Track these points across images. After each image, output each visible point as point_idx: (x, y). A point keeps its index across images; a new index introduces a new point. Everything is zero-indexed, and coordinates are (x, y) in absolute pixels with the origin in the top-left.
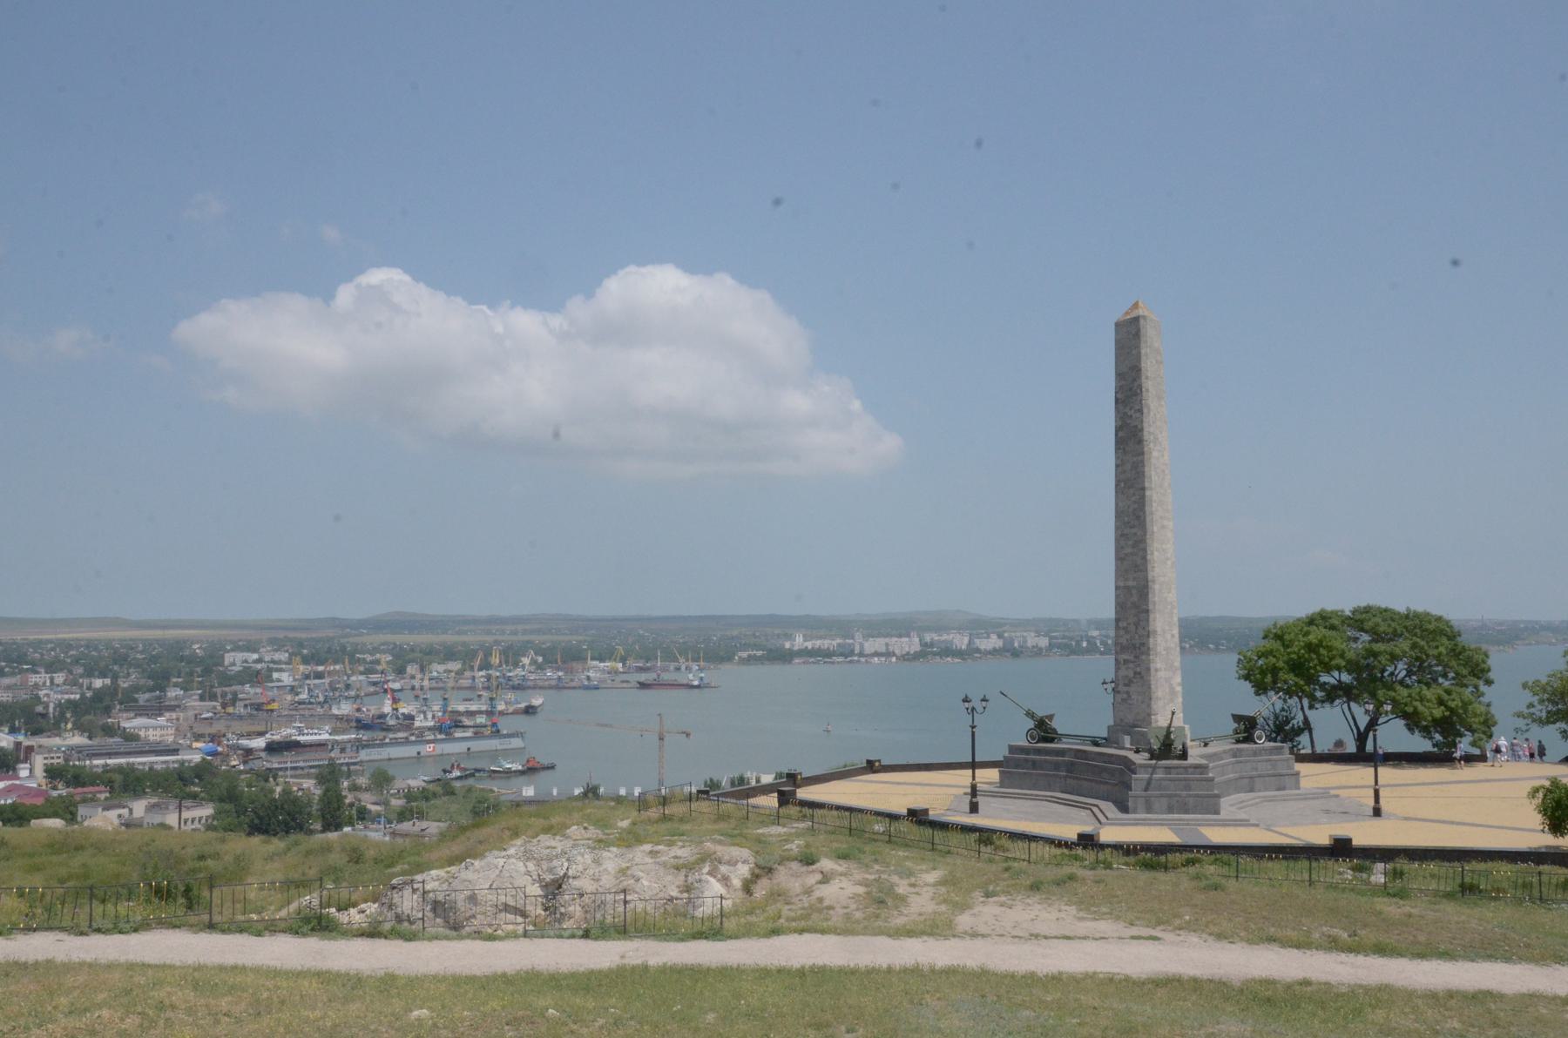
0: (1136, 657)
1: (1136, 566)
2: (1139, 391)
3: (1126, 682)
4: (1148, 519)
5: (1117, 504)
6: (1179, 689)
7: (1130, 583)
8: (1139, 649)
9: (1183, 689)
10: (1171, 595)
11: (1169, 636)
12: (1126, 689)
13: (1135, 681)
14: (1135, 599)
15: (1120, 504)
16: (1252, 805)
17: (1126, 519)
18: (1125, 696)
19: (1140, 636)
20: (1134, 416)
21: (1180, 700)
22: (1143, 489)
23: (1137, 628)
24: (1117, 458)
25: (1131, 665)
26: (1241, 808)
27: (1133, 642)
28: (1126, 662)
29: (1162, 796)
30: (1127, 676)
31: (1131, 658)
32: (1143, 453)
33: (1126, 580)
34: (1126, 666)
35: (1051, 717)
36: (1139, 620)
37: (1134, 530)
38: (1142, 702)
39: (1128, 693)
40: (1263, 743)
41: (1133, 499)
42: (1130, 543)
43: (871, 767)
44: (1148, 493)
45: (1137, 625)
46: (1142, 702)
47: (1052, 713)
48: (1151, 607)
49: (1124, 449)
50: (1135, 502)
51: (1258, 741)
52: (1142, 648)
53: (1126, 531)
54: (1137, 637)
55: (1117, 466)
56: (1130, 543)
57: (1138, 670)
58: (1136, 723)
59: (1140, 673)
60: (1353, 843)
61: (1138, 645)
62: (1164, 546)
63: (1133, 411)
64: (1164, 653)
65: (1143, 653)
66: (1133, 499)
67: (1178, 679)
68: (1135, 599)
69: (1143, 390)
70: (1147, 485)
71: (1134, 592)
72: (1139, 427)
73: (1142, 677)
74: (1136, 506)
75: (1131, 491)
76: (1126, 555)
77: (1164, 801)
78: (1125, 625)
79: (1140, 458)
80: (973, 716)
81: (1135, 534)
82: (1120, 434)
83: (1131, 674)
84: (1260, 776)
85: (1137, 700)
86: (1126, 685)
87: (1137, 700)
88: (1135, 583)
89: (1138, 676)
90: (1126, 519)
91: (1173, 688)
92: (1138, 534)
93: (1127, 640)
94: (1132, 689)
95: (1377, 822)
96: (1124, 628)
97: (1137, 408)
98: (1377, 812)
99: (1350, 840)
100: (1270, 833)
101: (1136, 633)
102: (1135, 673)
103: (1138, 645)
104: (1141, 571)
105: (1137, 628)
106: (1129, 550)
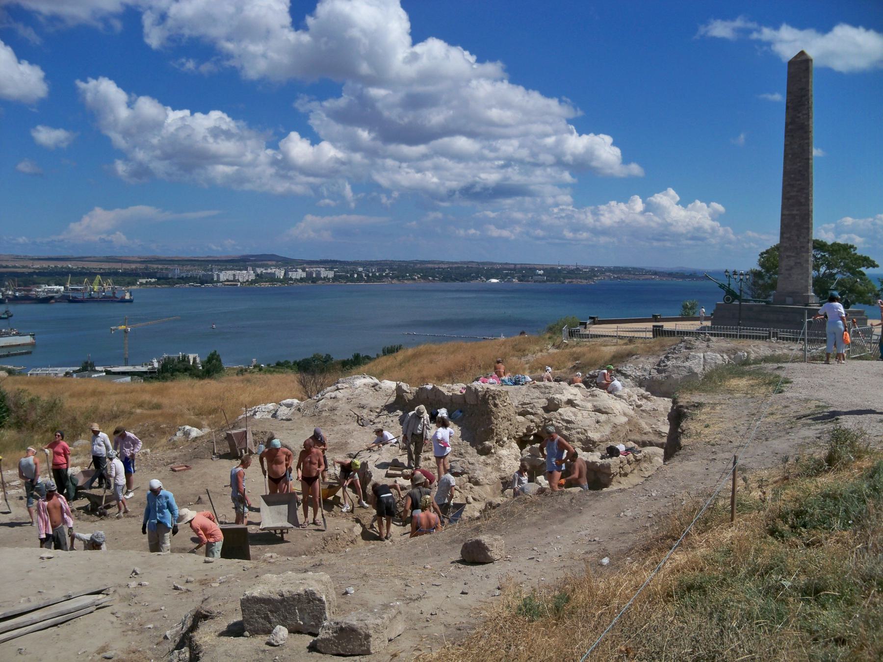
2: (806, 103)
4: (810, 176)
5: (785, 168)
7: (795, 212)
15: (788, 167)
17: (793, 176)
20: (802, 117)
22: (808, 159)
23: (798, 238)
24: (786, 140)
28: (788, 257)
31: (793, 254)
32: (808, 138)
37: (798, 183)
41: (799, 164)
44: (810, 161)
46: (801, 279)
48: (810, 226)
49: (792, 136)
50: (800, 166)
54: (798, 243)
55: (786, 145)
57: (798, 261)
59: (800, 263)
61: (799, 247)
66: (799, 164)
70: (810, 157)
72: (806, 123)
78: (788, 235)
79: (806, 141)
82: (790, 127)
86: (787, 270)
88: (798, 212)
90: (793, 176)
93: (790, 245)
96: (787, 238)
97: (804, 112)
102: (795, 263)
103: (799, 247)
105: (798, 238)
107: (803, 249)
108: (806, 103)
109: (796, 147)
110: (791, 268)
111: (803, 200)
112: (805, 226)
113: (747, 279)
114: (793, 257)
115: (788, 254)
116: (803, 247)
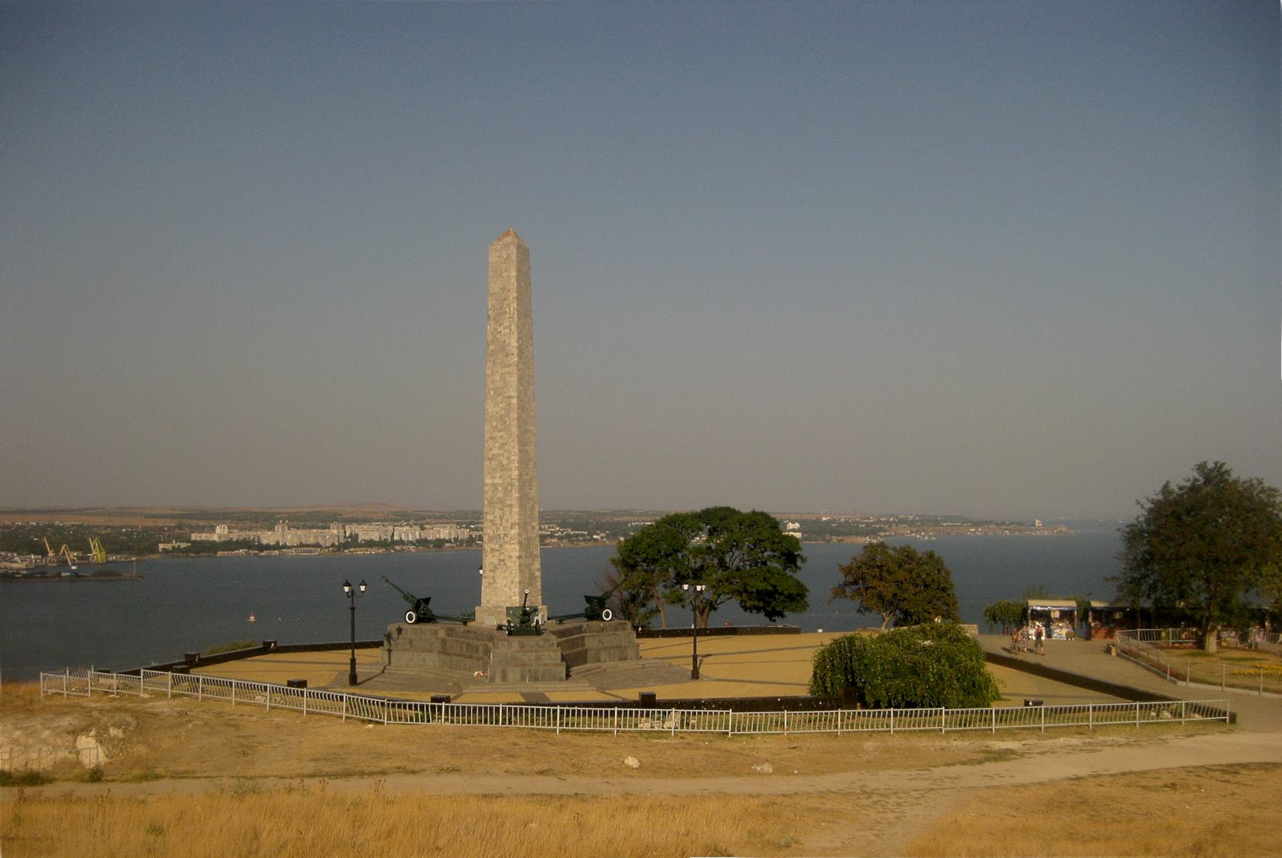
0: (500, 546)
1: (503, 466)
3: (492, 568)
6: (538, 574)
7: (497, 481)
8: (504, 539)
9: (542, 574)
10: (532, 492)
11: (529, 528)
12: (491, 574)
13: (499, 567)
14: (500, 495)
16: (592, 674)
18: (492, 580)
19: (503, 528)
20: (503, 332)
21: (539, 584)
23: (501, 521)
25: (497, 553)
26: (587, 676)
27: (499, 532)
29: (516, 666)
30: (492, 563)
33: (494, 478)
34: (493, 554)
35: (427, 601)
36: (504, 514)
37: (499, 434)
38: (505, 586)
39: (493, 578)
40: (610, 620)
41: (501, 405)
42: (497, 445)
43: (266, 649)
45: (501, 518)
46: (505, 586)
47: (428, 596)
50: (502, 408)
51: (606, 619)
52: (505, 538)
53: (493, 435)
56: (497, 445)
57: (502, 557)
58: (500, 604)
59: (503, 560)
60: (657, 699)
61: (502, 536)
62: (527, 448)
63: (502, 328)
64: (526, 542)
65: (506, 543)
66: (501, 405)
67: (537, 565)
68: (500, 495)
69: (512, 309)
71: (500, 488)
73: (505, 564)
74: (503, 412)
75: (500, 399)
76: (493, 455)
77: (518, 670)
78: (492, 518)
80: (353, 599)
81: (501, 437)
83: (496, 562)
84: (605, 648)
85: (501, 584)
86: (491, 571)
87: (501, 584)
89: (502, 563)
90: (494, 424)
91: (533, 574)
92: (505, 436)
94: (498, 572)
95: (695, 684)
96: (491, 521)
98: (695, 675)
99: (654, 696)
100: (603, 694)
101: (501, 525)
102: (499, 560)
103: (502, 536)
104: (506, 470)
105: (501, 521)
106: (495, 451)
107: (505, 538)
108: (508, 310)
109: (498, 378)
110: (496, 568)
111: (505, 462)
112: (508, 502)
113: (363, 592)
114: (498, 551)
115: (493, 546)
116: (506, 535)
